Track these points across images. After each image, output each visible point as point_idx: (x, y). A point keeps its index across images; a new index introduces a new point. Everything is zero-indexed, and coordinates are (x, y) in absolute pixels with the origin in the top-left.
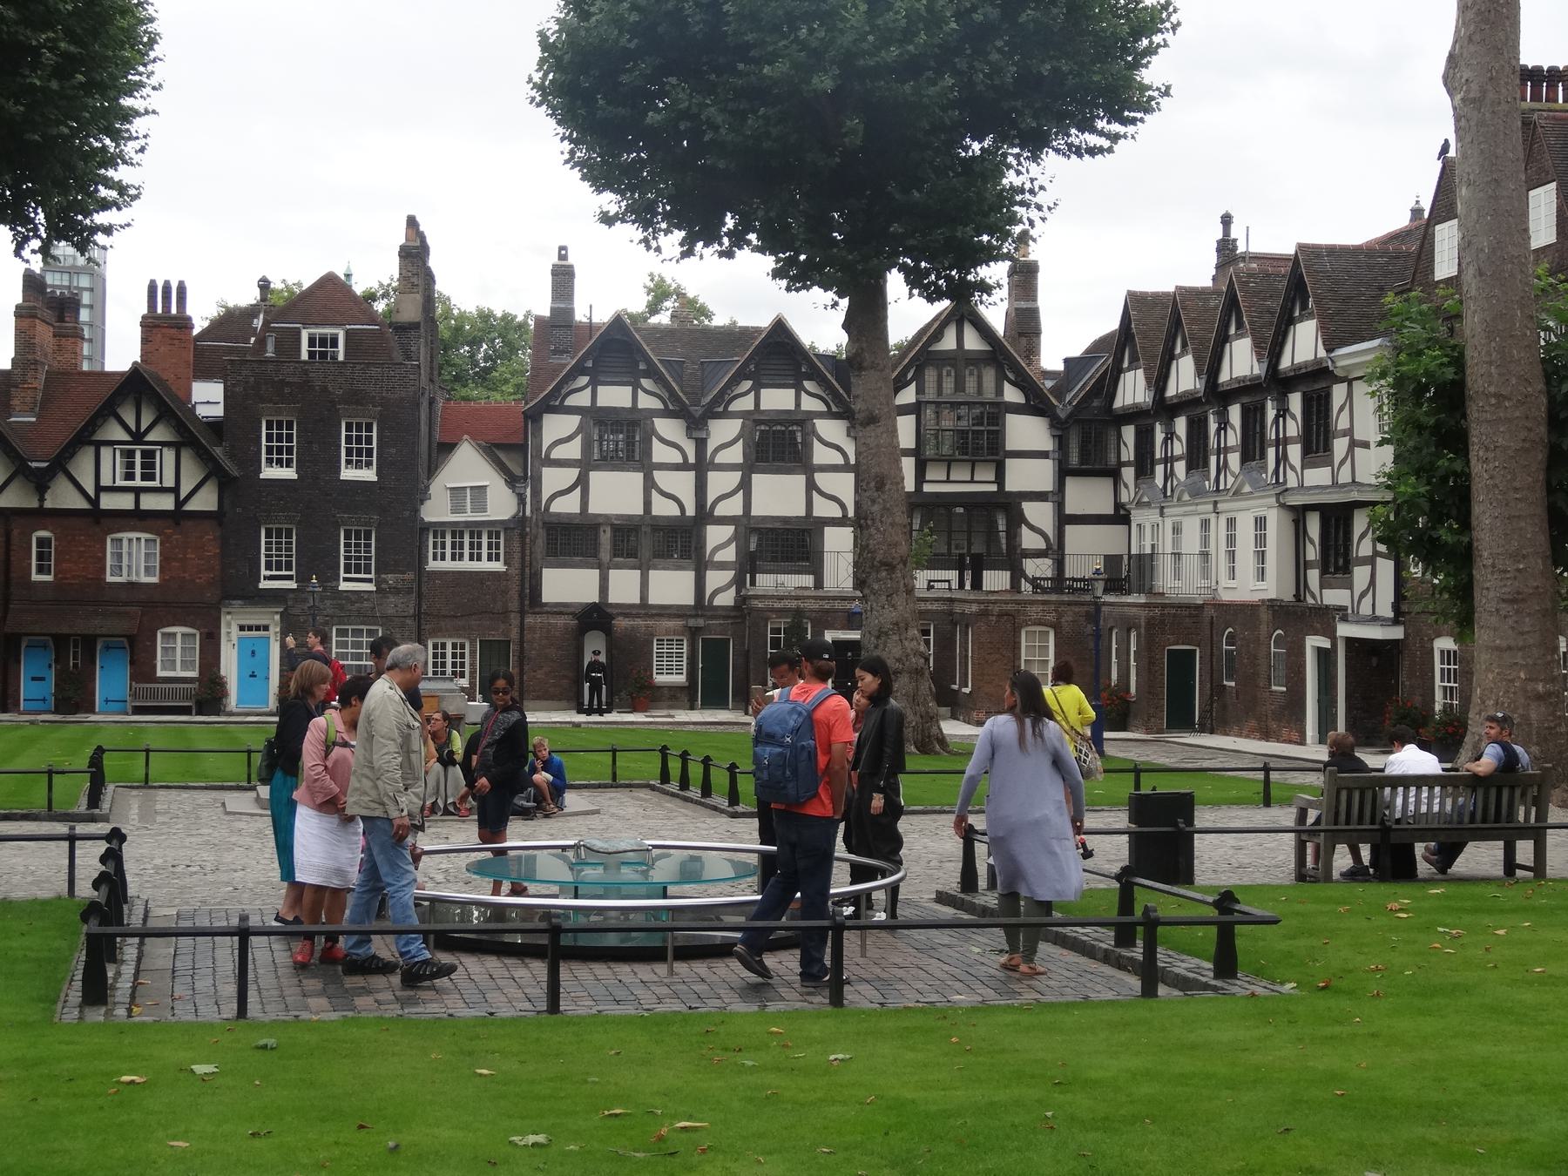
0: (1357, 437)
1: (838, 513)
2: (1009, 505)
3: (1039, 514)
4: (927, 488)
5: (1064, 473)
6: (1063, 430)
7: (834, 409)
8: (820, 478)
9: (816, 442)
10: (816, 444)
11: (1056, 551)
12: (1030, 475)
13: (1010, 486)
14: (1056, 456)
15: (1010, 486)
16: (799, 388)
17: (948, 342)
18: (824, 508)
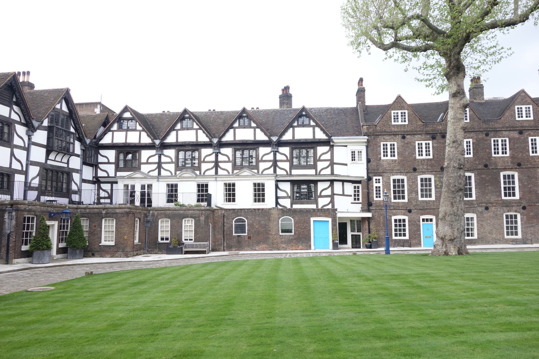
0: (335, 162)
1: (20, 168)
2: (68, 173)
3: (76, 177)
4: (49, 162)
5: (84, 163)
6: (86, 148)
7: (23, 121)
8: (16, 151)
9: (15, 134)
10: (15, 135)
11: (79, 192)
12: (75, 163)
13: (70, 166)
14: (82, 157)
15: (70, 166)
16: (11, 108)
17: (58, 106)
18: (16, 166)
